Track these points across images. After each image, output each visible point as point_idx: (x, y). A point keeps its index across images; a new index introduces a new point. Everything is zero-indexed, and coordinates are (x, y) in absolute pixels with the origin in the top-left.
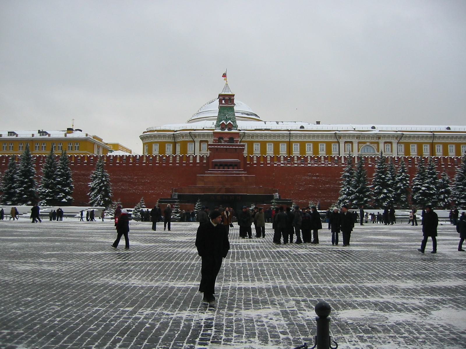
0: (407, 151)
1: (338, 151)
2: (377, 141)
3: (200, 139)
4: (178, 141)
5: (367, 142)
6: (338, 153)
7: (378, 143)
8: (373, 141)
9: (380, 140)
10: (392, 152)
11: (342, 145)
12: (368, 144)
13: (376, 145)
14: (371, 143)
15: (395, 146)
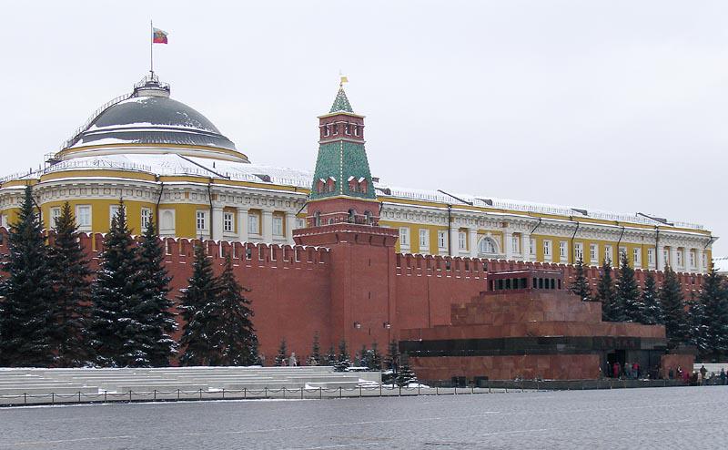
0: (541, 251)
1: (447, 247)
2: (501, 229)
3: (224, 204)
4: (167, 201)
5: (487, 231)
6: (447, 250)
7: (502, 234)
8: (495, 229)
9: (506, 229)
10: (284, 236)
11: (455, 234)
12: (489, 235)
13: (499, 237)
14: (494, 233)
15: (526, 240)
